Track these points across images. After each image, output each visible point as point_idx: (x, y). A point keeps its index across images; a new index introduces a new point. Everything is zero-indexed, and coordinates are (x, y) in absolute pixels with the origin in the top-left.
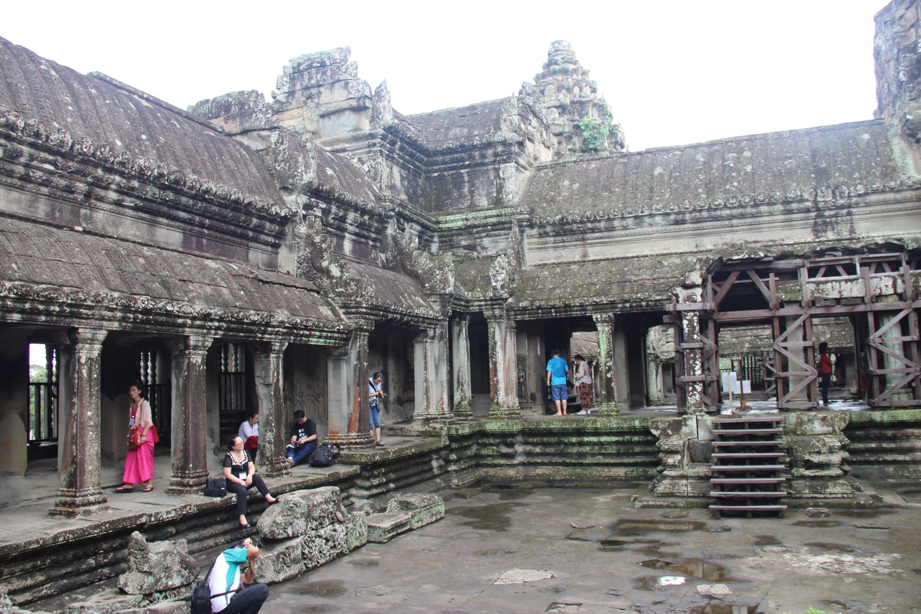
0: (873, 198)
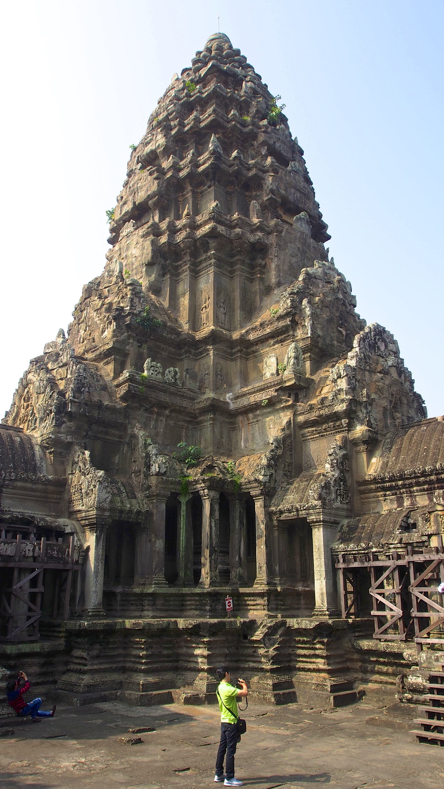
0: (19, 484)
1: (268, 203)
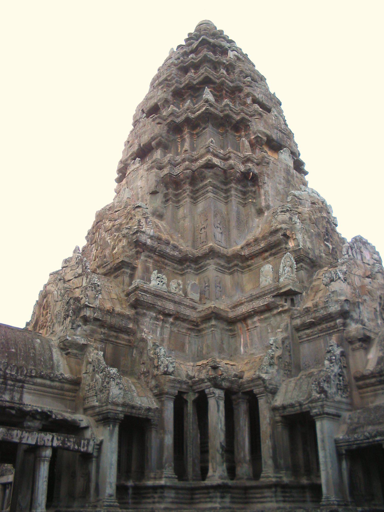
0: (39, 380)
1: (254, 141)
